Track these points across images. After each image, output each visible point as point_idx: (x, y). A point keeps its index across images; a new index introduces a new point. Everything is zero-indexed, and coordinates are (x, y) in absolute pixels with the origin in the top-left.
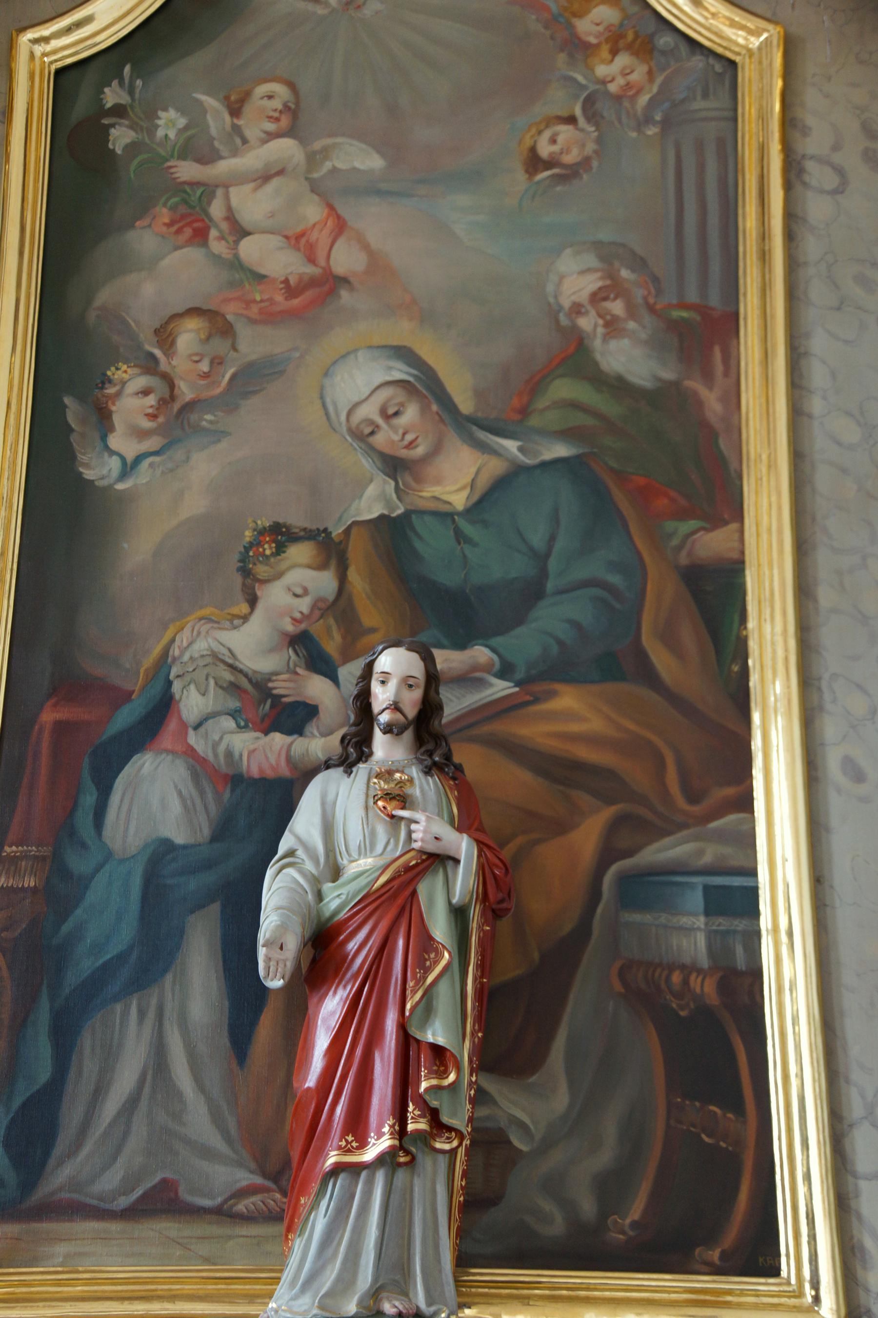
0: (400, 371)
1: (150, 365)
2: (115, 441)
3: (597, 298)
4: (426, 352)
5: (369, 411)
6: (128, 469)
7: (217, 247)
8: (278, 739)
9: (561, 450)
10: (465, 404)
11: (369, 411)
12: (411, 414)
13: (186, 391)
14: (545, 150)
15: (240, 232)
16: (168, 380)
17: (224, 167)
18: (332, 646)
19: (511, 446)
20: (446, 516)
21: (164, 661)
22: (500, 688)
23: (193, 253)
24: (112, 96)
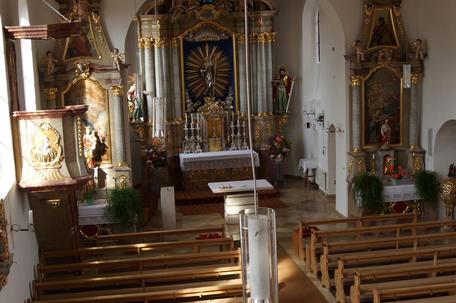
0: (383, 99)
1: (370, 99)
2: (369, 104)
3: (393, 94)
4: (385, 98)
5: (381, 101)
6: (370, 105)
7: (373, 91)
8: (378, 120)
9: (391, 103)
10: (386, 100)
11: (381, 101)
12: (384, 101)
13: (372, 101)
14: (390, 84)
15: (375, 90)
16: (371, 100)
17: (374, 86)
18: (380, 115)
19: (389, 103)
20: (385, 107)
21: (372, 116)
22: (388, 117)
23: (372, 92)
24: (367, 82)
